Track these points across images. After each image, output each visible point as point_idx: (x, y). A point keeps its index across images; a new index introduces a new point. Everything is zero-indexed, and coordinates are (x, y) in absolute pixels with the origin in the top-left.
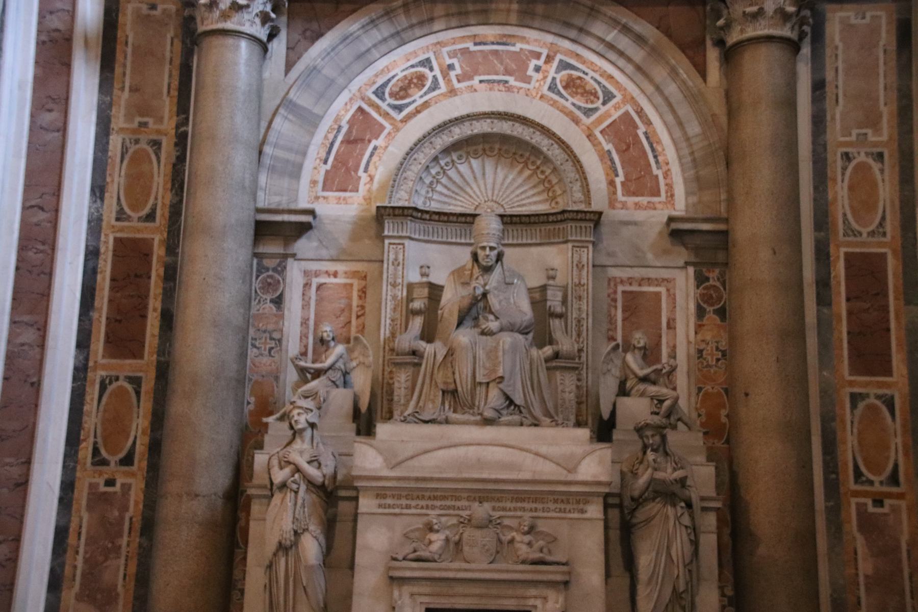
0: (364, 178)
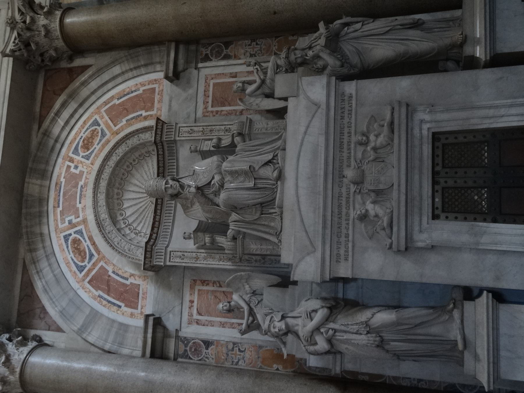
0: (131, 280)
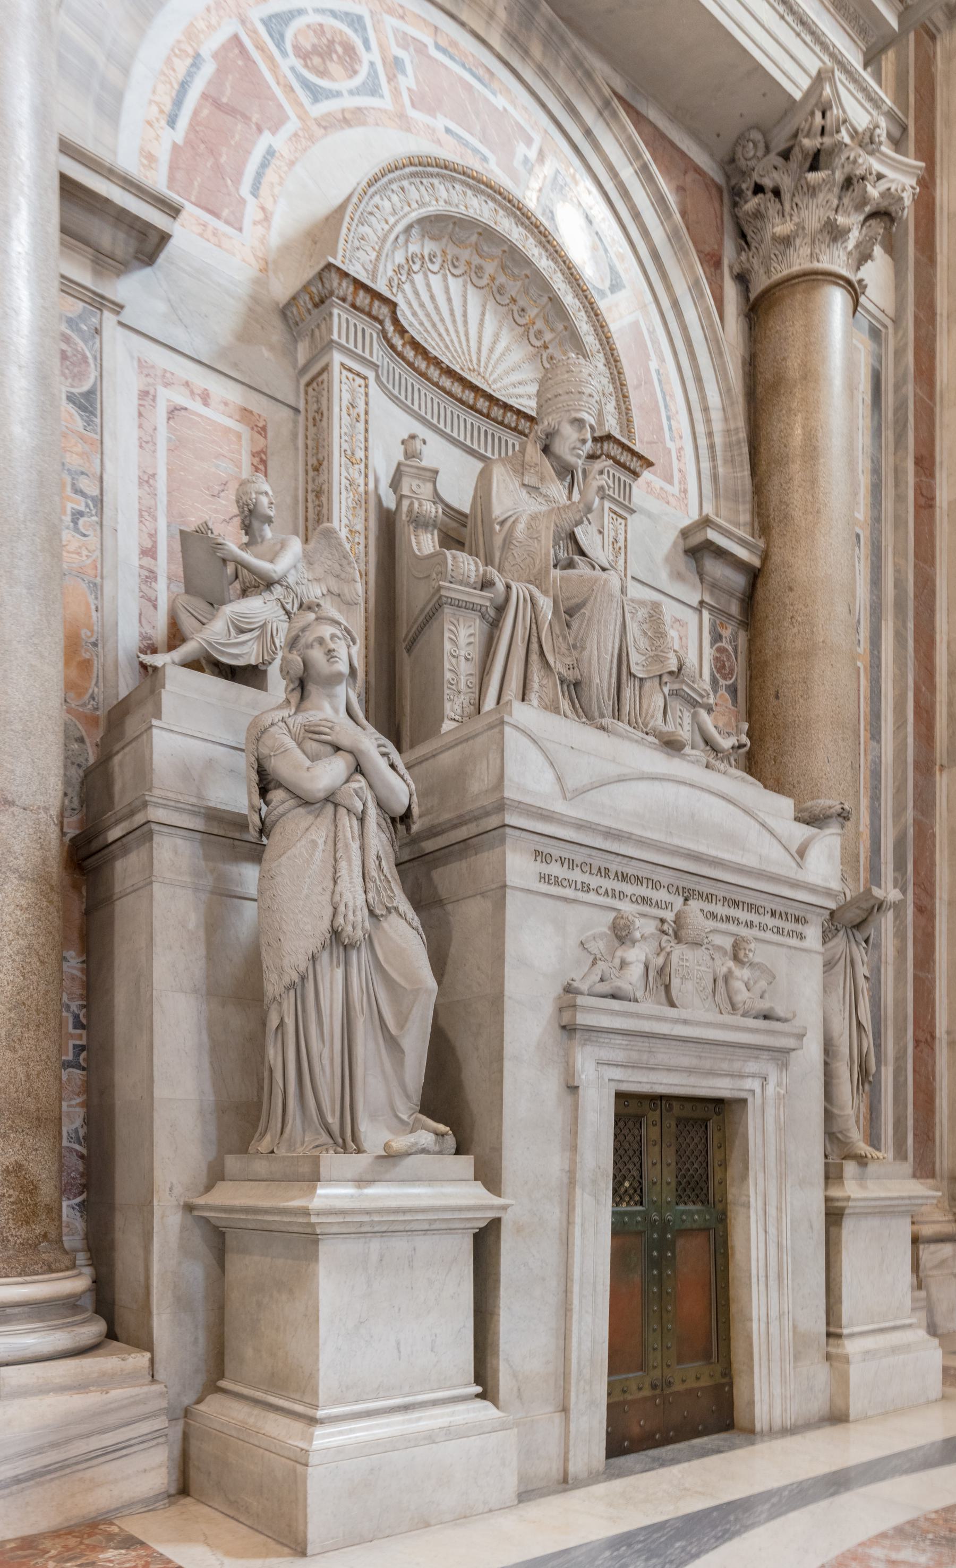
0: (251, 211)
